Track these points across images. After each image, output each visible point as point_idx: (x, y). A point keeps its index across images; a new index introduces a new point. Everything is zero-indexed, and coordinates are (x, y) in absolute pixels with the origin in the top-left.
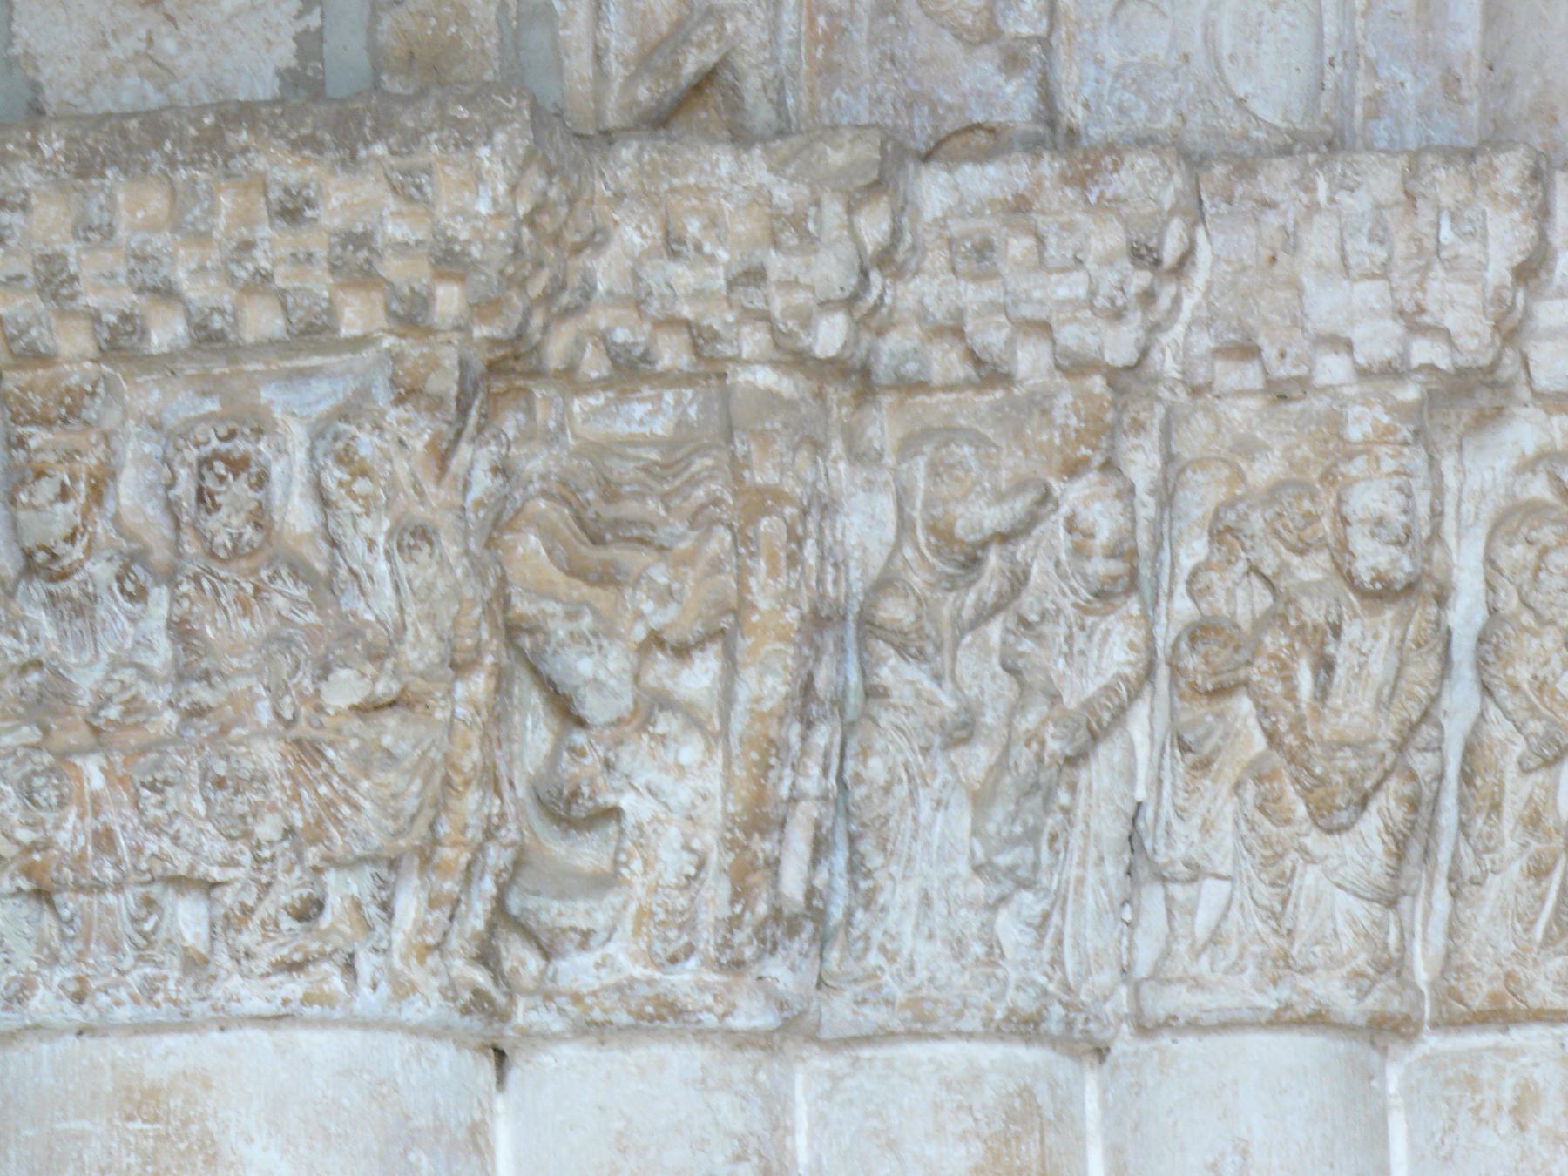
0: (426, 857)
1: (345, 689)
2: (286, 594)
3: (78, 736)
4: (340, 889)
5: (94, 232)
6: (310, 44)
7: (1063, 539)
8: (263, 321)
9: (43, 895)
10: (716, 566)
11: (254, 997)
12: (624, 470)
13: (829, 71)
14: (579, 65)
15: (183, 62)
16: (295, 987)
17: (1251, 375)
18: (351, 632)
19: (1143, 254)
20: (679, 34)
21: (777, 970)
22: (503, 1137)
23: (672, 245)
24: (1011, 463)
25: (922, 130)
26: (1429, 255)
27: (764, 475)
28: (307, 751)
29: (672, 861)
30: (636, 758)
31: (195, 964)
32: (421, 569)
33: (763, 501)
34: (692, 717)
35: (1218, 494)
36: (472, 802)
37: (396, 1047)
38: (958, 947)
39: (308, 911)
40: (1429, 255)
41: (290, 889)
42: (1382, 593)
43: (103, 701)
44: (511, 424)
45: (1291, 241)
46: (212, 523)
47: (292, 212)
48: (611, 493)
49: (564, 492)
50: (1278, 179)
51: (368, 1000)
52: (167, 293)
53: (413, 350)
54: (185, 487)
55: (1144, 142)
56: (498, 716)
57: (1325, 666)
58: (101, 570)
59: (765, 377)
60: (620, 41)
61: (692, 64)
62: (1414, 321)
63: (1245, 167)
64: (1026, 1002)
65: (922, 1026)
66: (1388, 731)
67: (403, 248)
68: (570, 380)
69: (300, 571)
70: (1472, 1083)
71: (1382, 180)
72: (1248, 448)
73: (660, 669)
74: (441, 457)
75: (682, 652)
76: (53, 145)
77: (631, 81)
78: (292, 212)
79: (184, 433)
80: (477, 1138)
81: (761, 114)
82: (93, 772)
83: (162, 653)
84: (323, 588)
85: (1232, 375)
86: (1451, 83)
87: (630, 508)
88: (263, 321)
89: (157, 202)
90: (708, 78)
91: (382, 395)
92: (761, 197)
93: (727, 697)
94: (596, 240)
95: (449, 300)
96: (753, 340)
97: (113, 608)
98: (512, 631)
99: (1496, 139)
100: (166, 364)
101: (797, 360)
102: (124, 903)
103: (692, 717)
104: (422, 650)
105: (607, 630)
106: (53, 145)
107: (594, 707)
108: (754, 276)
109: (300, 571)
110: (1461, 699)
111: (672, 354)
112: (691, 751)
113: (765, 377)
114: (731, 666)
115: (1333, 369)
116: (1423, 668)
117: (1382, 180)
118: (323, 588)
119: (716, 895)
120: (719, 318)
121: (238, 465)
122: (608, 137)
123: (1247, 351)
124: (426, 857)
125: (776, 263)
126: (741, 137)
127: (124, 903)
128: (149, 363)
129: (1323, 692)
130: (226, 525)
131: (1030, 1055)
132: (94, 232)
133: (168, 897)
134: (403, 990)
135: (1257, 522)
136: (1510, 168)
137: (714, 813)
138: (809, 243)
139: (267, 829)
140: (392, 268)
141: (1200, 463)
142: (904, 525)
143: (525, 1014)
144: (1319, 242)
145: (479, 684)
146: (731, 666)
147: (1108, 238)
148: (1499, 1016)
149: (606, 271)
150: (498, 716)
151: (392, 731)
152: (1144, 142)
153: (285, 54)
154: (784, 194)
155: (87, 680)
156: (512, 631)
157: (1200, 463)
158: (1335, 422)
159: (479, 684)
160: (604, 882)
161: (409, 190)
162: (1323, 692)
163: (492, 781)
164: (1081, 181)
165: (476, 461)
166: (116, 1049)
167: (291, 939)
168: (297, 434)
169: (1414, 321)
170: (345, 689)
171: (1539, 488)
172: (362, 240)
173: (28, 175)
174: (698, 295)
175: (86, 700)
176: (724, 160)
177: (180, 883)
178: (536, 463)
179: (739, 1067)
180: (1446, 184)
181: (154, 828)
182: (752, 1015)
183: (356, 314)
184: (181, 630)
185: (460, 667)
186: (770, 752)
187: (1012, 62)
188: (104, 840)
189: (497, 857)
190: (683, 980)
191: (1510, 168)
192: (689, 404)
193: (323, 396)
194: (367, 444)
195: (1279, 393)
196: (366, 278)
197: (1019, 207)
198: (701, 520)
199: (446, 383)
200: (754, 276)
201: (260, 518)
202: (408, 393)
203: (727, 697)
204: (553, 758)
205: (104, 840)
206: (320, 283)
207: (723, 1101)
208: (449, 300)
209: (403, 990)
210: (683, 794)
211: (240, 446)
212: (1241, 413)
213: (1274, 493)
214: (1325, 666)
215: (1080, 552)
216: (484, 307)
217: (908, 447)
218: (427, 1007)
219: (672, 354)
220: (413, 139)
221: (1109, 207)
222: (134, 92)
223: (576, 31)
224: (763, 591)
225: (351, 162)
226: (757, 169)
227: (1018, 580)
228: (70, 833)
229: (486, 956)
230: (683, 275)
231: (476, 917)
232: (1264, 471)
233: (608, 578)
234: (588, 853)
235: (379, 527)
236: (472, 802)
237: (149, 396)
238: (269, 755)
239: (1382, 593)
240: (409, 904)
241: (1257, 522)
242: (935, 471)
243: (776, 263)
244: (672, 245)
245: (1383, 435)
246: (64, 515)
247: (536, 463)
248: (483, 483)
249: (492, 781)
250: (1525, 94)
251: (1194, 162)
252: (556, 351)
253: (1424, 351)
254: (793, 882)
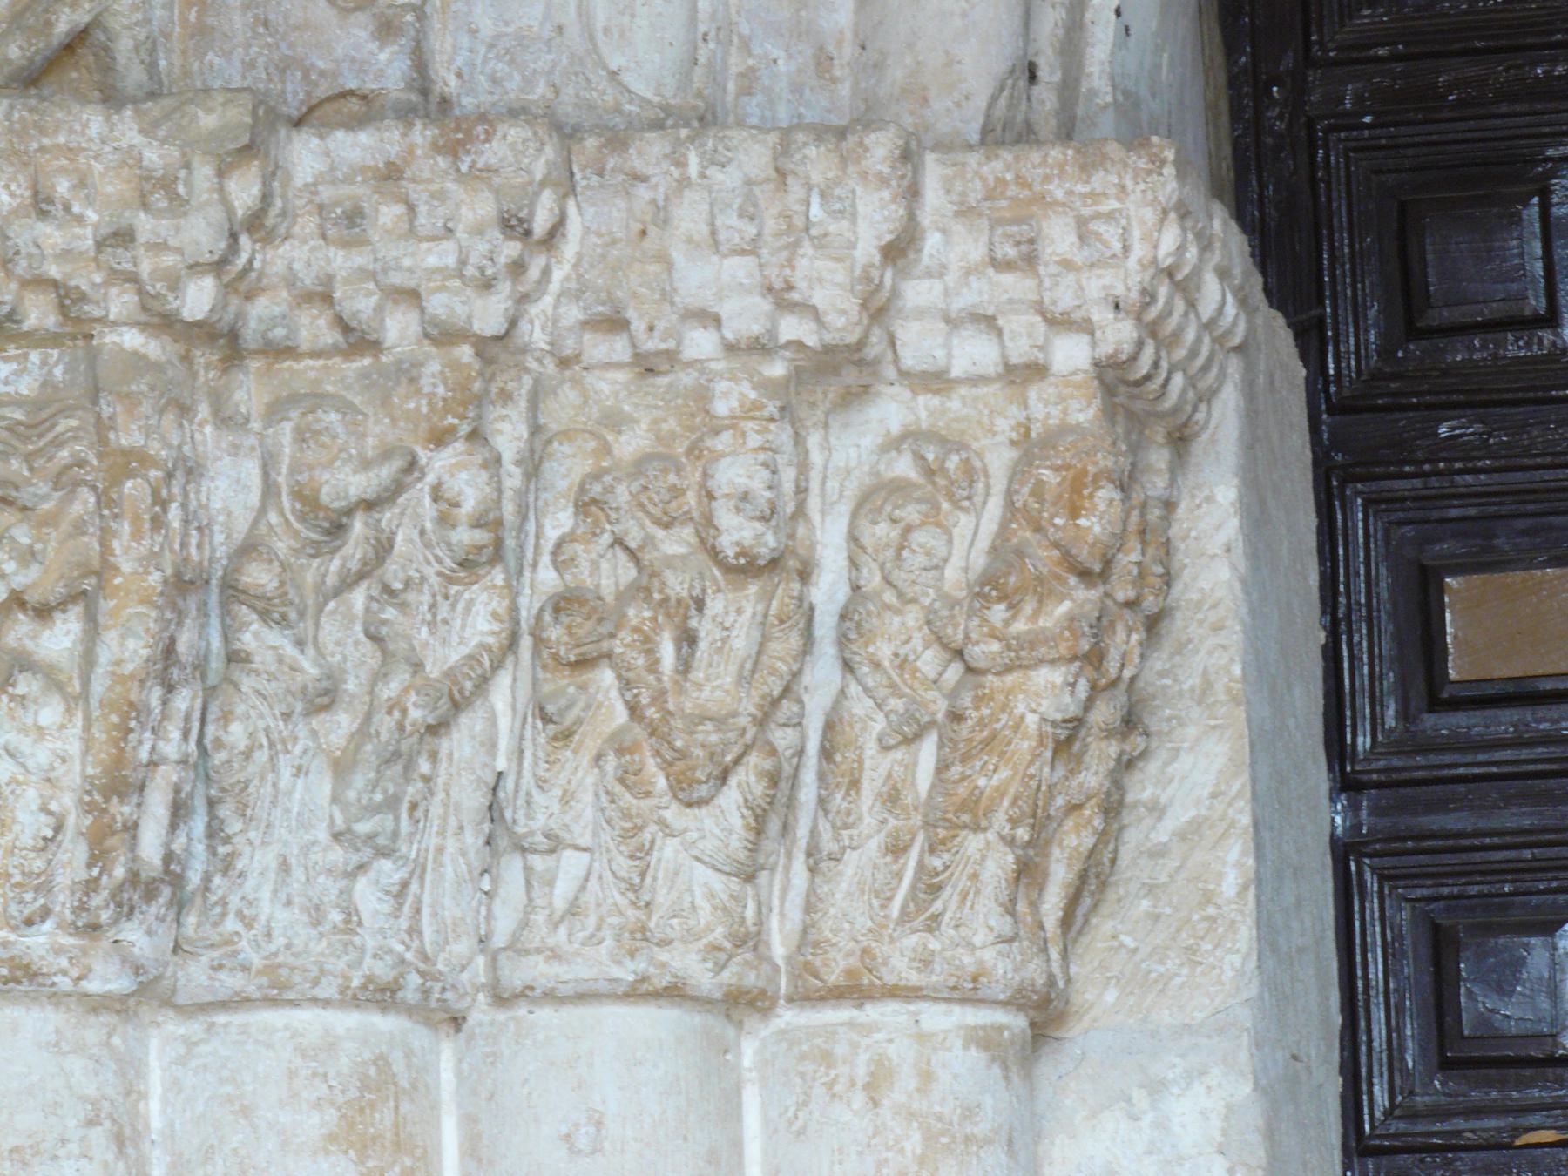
7: (428, 509)
10: (79, 528)
13: (202, 34)
17: (619, 348)
19: (513, 225)
21: (133, 934)
24: (378, 430)
25: (294, 94)
26: (798, 233)
27: (129, 437)
33: (129, 463)
34: (52, 678)
35: (587, 466)
38: (316, 915)
40: (798, 233)
42: (746, 568)
45: (661, 215)
50: (650, 152)
55: (517, 112)
57: (688, 639)
59: (132, 339)
62: (782, 298)
63: (617, 141)
64: (382, 970)
65: (278, 994)
66: (749, 706)
70: (827, 1058)
71: (754, 157)
72: (615, 421)
75: (43, 613)
81: (133, 75)
85: (601, 348)
86: (823, 62)
90: (79, 39)
92: (131, 158)
93: (88, 659)
96: (120, 302)
99: (867, 118)
101: (164, 322)
103: (52, 678)
108: (123, 237)
110: (822, 676)
111: (39, 313)
112: (50, 713)
113: (132, 339)
114: (92, 628)
115: (700, 343)
116: (785, 644)
117: (754, 157)
119: (73, 858)
120: (87, 279)
123: (615, 323)
125: (145, 225)
126: (112, 98)
129: (685, 666)
131: (386, 1023)
135: (622, 495)
136: (880, 148)
137: (71, 776)
138: (179, 205)
141: (567, 435)
142: (269, 490)
144: (689, 216)
146: (92, 628)
147: (479, 207)
148: (853, 992)
152: (517, 112)
154: (154, 156)
157: (567, 435)
158: (703, 396)
162: (685, 666)
164: (453, 150)
169: (782, 298)
171: (903, 467)
174: (66, 255)
176: (94, 121)
179: (93, 1031)
180: (816, 161)
182: (107, 979)
186: (129, 716)
187: (386, 30)
190: (38, 943)
191: (880, 148)
192: (54, 364)
195: (647, 366)
197: (390, 175)
198: (66, 481)
200: (123, 237)
203: (88, 659)
207: (76, 1065)
210: (41, 756)
212: (608, 386)
213: (640, 465)
214: (688, 639)
215: (445, 521)
217: (275, 411)
219: (39, 313)
221: (481, 176)
224: (126, 554)
226: (128, 130)
227: (383, 548)
230: (51, 235)
232: (630, 444)
239: (746, 568)
241: (622, 495)
242: (301, 437)
243: (145, 225)
245: (750, 411)
250: (896, 74)
251: (567, 134)
253: (792, 328)
254: (151, 846)
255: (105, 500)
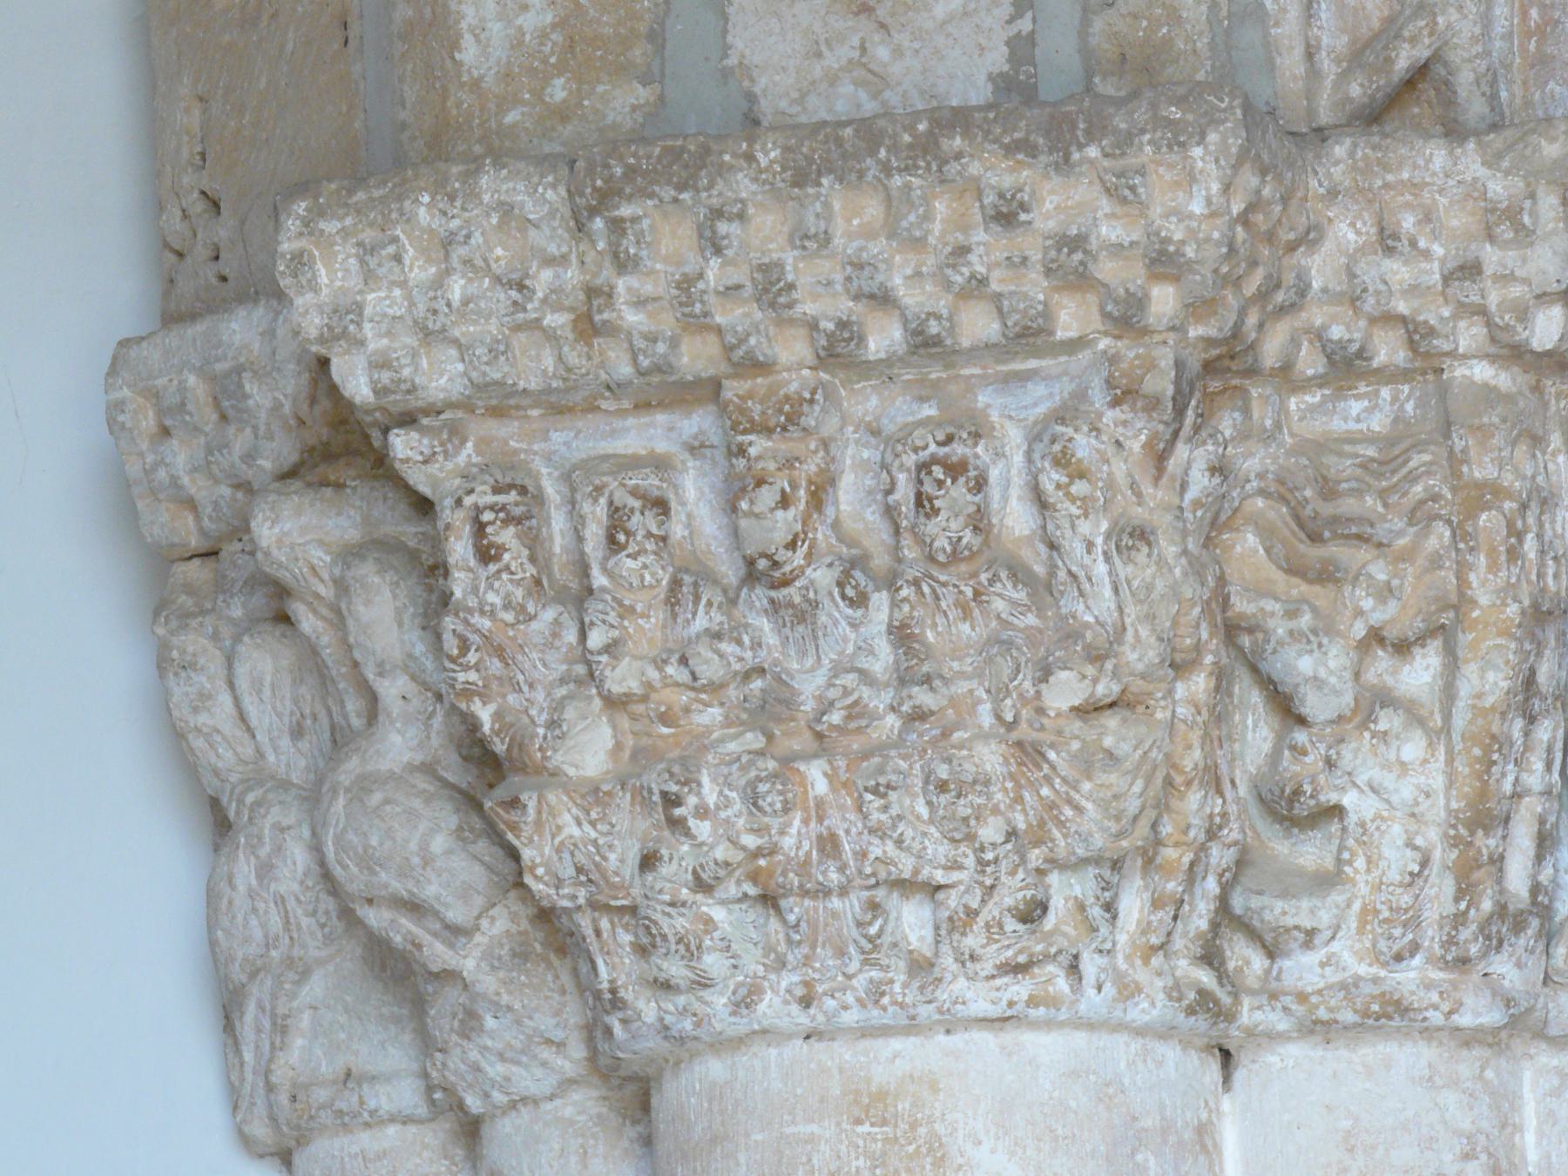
0: (1149, 858)
1: (1065, 691)
2: (1005, 597)
3: (801, 742)
4: (1064, 890)
5: (811, 241)
6: (1022, 48)
8: (979, 325)
9: (769, 901)
10: (1436, 562)
11: (980, 1000)
12: (1342, 467)
14: (1291, 63)
15: (896, 69)
16: (1020, 989)
18: (1071, 633)
20: (1391, 30)
21: (1503, 967)
22: (1230, 1137)
23: (1387, 241)
27: (1482, 470)
28: (1029, 753)
29: (1396, 859)
30: (1358, 755)
31: (921, 967)
32: (1139, 571)
33: (1483, 495)
34: (1413, 713)
36: (1194, 800)
37: (1122, 1048)
39: (1033, 912)
41: (1013, 890)
43: (826, 707)
44: (1227, 423)
46: (932, 527)
47: (1007, 215)
48: (1329, 490)
49: (1281, 490)
51: (1092, 1001)
52: (883, 299)
53: (1129, 351)
54: (904, 492)
56: (1218, 715)
58: (822, 577)
59: (1482, 372)
60: (1332, 38)
61: (1404, 59)
67: (1117, 249)
68: (1286, 377)
69: (1019, 574)
73: (1381, 665)
74: (1159, 457)
75: (1403, 648)
76: (769, 154)
77: (1343, 77)
78: (1007, 215)
79: (901, 439)
80: (1204, 1138)
81: (1475, 108)
82: (816, 777)
83: (883, 658)
84: (1042, 590)
87: (1348, 506)
88: (979, 325)
89: (873, 209)
90: (1421, 71)
91: (1098, 397)
92: (1474, 190)
93: (1449, 693)
94: (1311, 237)
95: (1164, 300)
96: (1469, 335)
97: (835, 614)
98: (1231, 630)
100: (884, 370)
101: (1514, 353)
102: (849, 907)
103: (1413, 713)
104: (1140, 652)
105: (1326, 627)
106: (769, 154)
107: (1314, 705)
108: (1470, 270)
109: (1019, 574)
111: (1388, 350)
112: (1412, 748)
113: (1482, 372)
114: (1452, 663)
118: (1042, 590)
119: (1440, 894)
120: (1435, 313)
121: (956, 469)
122: (1321, 134)
124: (1149, 858)
125: (1491, 257)
126: (1454, 132)
127: (849, 907)
128: (867, 369)
130: (945, 529)
132: (811, 241)
133: (893, 901)
134: (1128, 991)
137: (1436, 810)
138: (1525, 235)
139: (990, 832)
140: (1107, 270)
143: (1249, 1014)
145: (1199, 684)
146: (1452, 663)
149: (1320, 269)
150: (1218, 715)
151: (1113, 732)
153: (998, 58)
154: (1498, 188)
155: (809, 686)
156: (1231, 630)
159: (1199, 684)
160: (1328, 880)
161: (1123, 192)
163: (1214, 781)
165: (1192, 460)
166: (843, 1052)
167: (1016, 941)
168: (1014, 437)
170: (1065, 691)
172: (1076, 243)
173: (744, 185)
174: (1413, 290)
175: (809, 706)
176: (1437, 155)
177: (905, 886)
178: (1253, 462)
179: (1466, 1064)
181: (878, 831)
182: (1479, 1012)
183: (1071, 318)
184: (902, 635)
185: (1180, 667)
186: (1492, 749)
188: (829, 845)
189: (1220, 856)
190: (1408, 978)
192: (1409, 400)
193: (1039, 399)
194: (1084, 446)
196: (1081, 281)
198: (1421, 516)
199: (1162, 384)
200: (1470, 270)
201: (979, 521)
202: (1124, 394)
203: (1449, 693)
204: (1275, 757)
205: (829, 845)
206: (1035, 286)
207: (1450, 1099)
208: (1164, 300)
209: (1128, 991)
210: (1405, 791)
211: (958, 450)
216: (1199, 307)
218: (1152, 1007)
219: (1388, 350)
220: (1126, 141)
222: (849, 100)
223: (1288, 29)
224: (1483, 587)
225: (1064, 165)
226: (1471, 163)
228: (795, 838)
229: (1210, 957)
230: (1398, 271)
231: (1200, 917)
233: (1327, 575)
234: (1311, 852)
235: (1097, 528)
236: (1194, 800)
237: (867, 402)
238: (991, 758)
240: (1133, 904)
243: (1491, 257)
244: (1387, 241)
246: (785, 522)
247: (1253, 462)
248: (1200, 482)
249: (1214, 781)
252: (1272, 349)
254: (1517, 878)
255: (1460, 533)
